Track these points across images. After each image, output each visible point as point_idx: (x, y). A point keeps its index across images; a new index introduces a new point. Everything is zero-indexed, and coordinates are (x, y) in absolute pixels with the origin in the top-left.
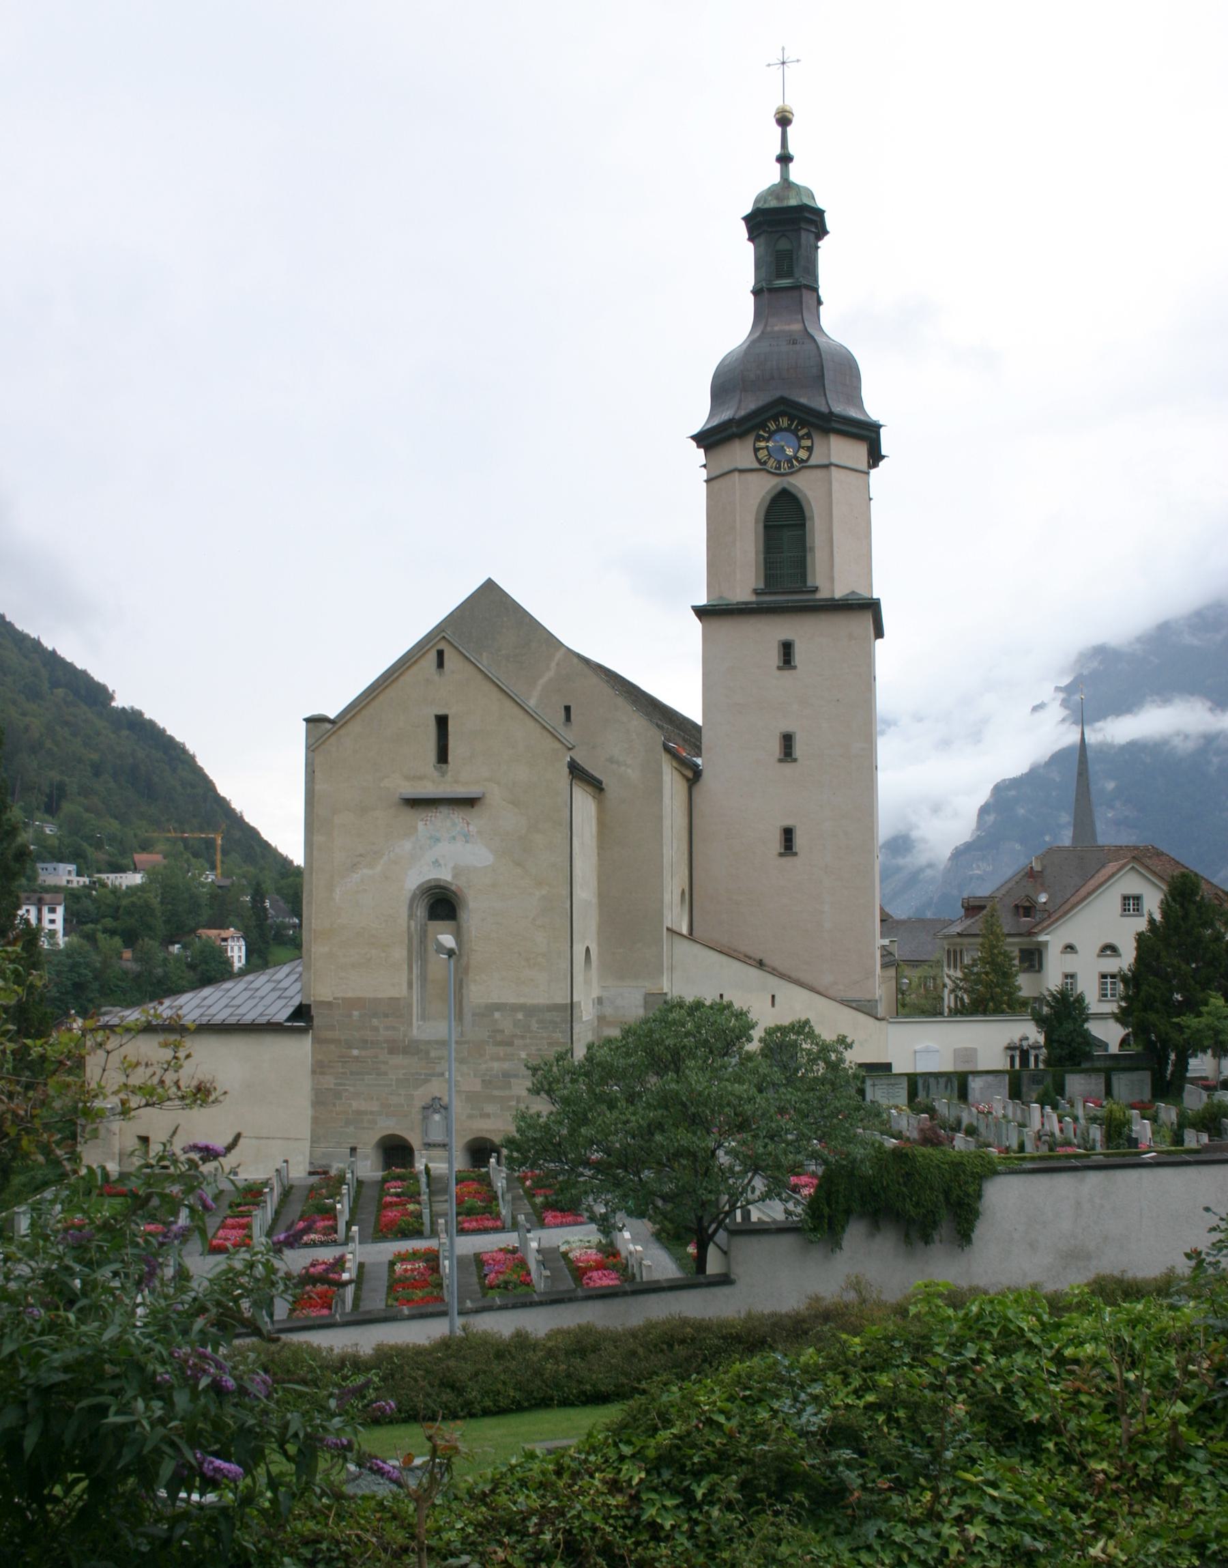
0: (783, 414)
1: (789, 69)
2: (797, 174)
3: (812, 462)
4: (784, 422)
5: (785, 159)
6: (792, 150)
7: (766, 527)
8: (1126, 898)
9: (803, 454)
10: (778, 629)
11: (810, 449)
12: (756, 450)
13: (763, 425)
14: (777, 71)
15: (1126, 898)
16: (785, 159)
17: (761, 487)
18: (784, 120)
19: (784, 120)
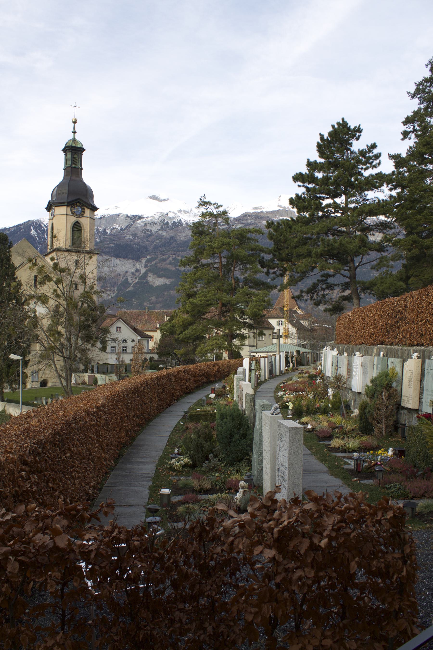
0: (79, 202)
1: (77, 109)
2: (78, 137)
3: (85, 215)
4: (78, 204)
5: (74, 132)
6: (76, 130)
7: (73, 230)
8: (117, 328)
9: (82, 213)
10: (75, 257)
11: (84, 212)
12: (71, 210)
13: (73, 204)
14: (73, 108)
15: (117, 328)
16: (74, 132)
17: (73, 219)
18: (75, 122)
19: (75, 122)
